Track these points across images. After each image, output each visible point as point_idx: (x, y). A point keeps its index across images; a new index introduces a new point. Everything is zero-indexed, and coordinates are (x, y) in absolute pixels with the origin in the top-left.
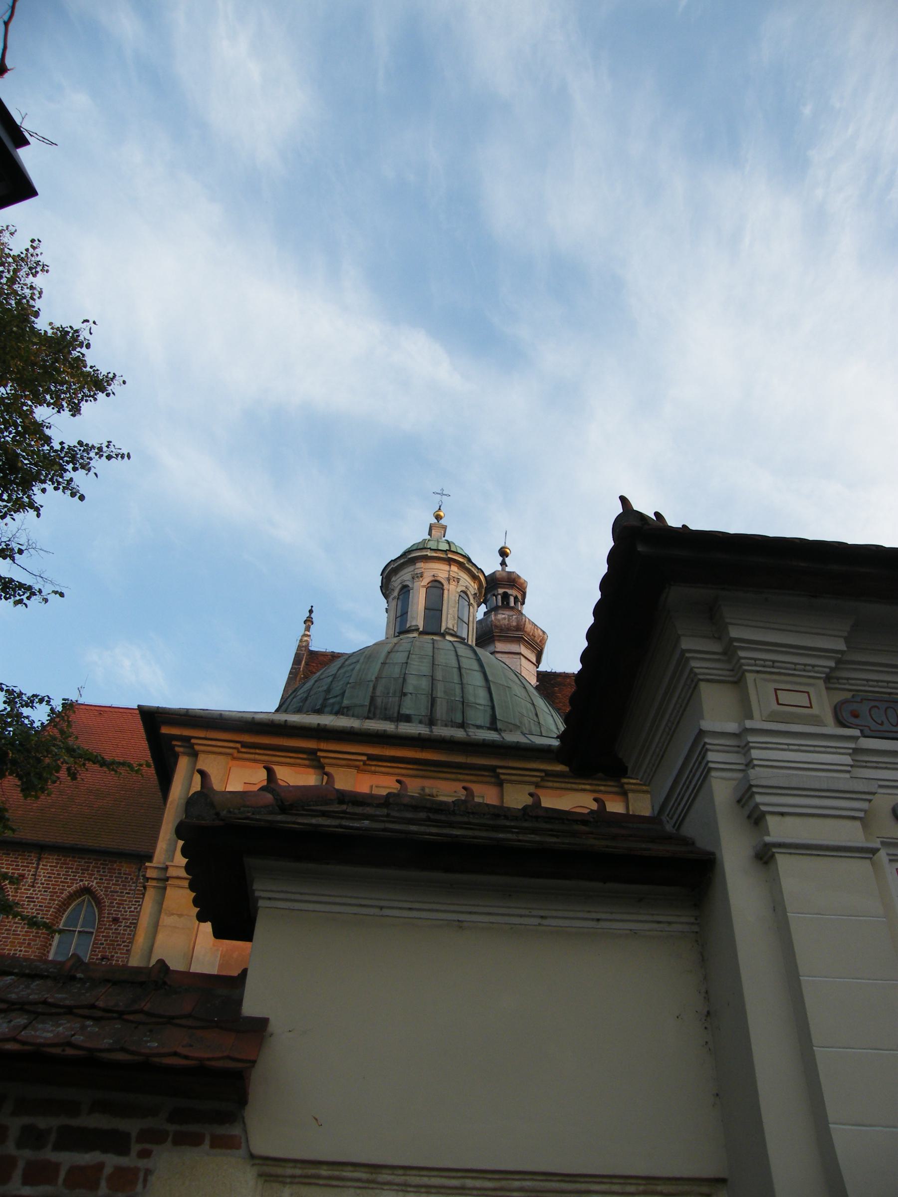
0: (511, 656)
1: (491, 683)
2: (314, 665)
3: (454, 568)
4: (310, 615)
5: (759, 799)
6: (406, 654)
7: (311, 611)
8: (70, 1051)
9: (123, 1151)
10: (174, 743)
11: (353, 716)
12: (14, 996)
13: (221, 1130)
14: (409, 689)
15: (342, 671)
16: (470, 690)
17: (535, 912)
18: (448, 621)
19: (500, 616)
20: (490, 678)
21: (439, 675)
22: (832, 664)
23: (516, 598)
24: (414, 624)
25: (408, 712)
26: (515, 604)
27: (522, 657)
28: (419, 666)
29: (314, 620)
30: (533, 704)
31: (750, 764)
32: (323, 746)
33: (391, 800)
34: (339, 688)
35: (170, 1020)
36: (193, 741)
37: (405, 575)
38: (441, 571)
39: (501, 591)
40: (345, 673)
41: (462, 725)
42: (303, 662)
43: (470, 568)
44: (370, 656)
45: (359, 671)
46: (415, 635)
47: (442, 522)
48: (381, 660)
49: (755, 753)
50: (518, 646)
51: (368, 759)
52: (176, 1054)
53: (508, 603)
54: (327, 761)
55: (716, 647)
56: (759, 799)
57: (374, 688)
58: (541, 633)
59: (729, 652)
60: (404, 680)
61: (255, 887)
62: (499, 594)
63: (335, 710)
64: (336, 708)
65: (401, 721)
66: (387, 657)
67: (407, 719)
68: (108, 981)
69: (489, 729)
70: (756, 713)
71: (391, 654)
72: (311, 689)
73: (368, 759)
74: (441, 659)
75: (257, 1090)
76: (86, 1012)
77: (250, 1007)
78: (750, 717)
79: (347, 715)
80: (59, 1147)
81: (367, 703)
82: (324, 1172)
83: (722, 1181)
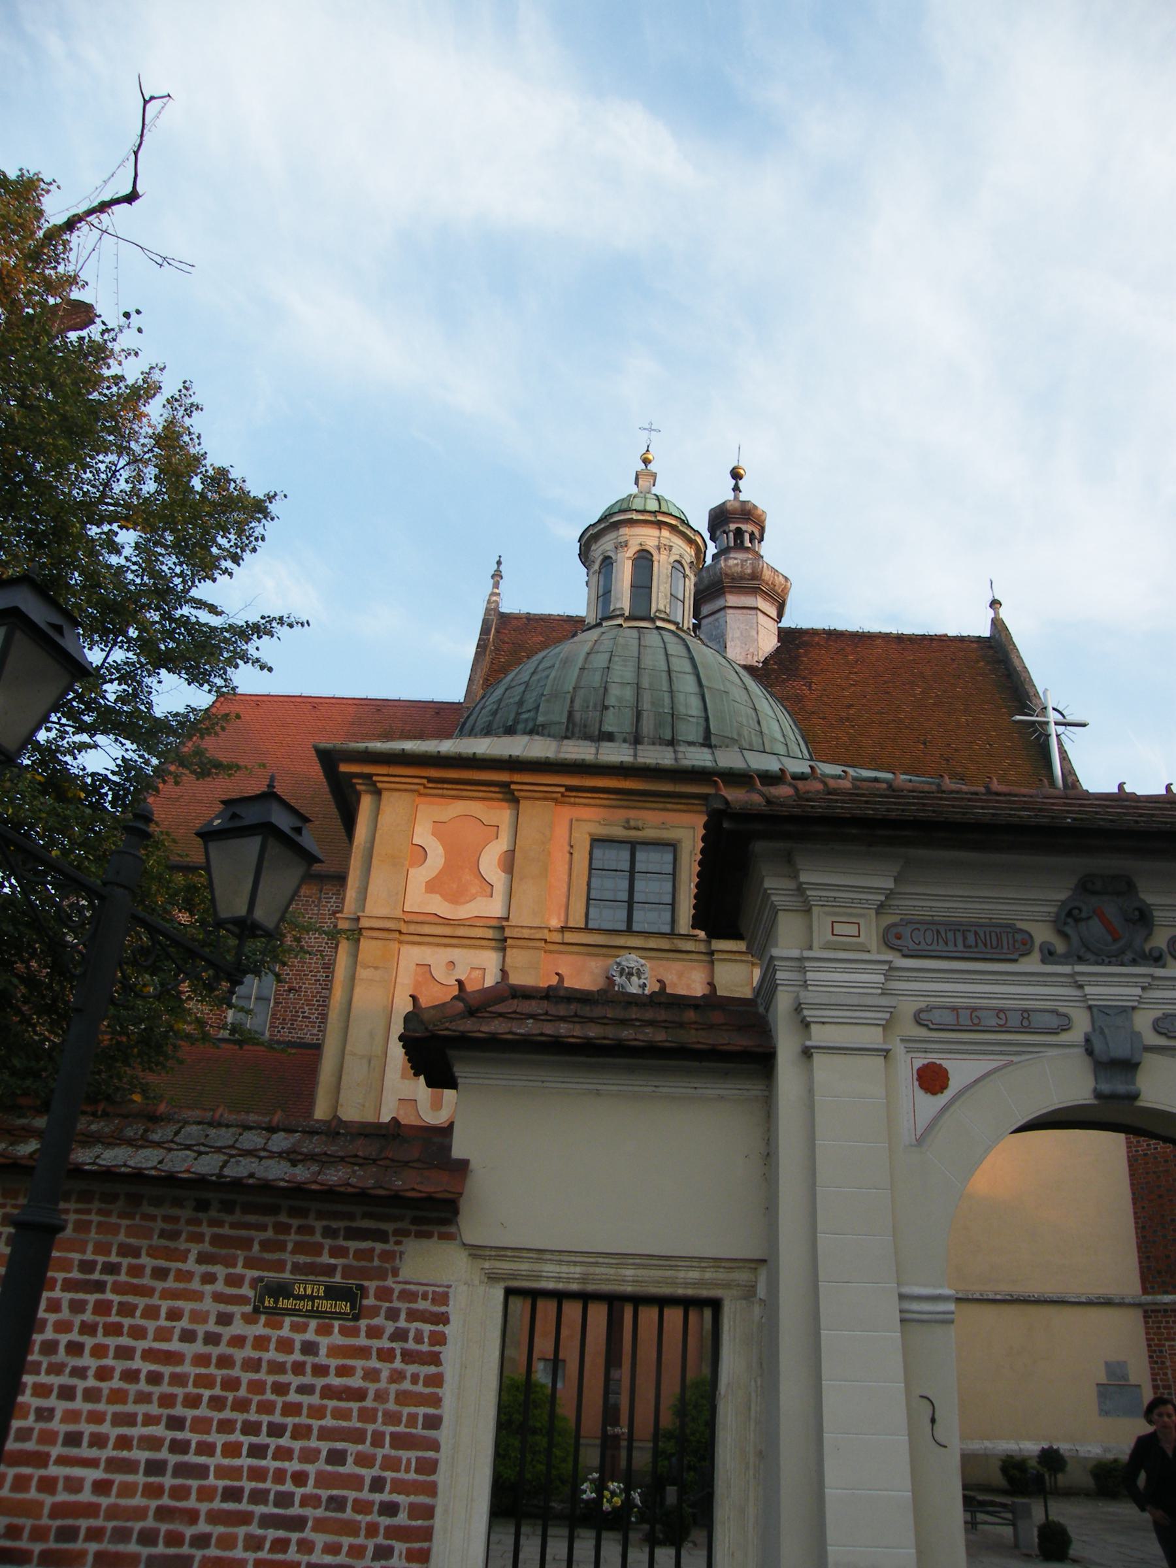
0: (745, 611)
1: (706, 690)
2: (507, 632)
3: (665, 533)
4: (498, 567)
5: (806, 1012)
6: (607, 656)
7: (499, 563)
8: (350, 1190)
9: (386, 1241)
10: (355, 781)
11: (549, 736)
12: (305, 1150)
13: (443, 1229)
14: (611, 701)
15: (535, 678)
16: (680, 698)
17: (650, 1083)
18: (660, 601)
19: (731, 562)
20: (704, 682)
21: (645, 683)
22: (882, 898)
23: (752, 535)
24: (618, 606)
25: (610, 729)
26: (751, 542)
27: (759, 612)
28: (623, 672)
29: (503, 574)
30: (755, 709)
31: (805, 985)
32: (517, 778)
33: (551, 993)
34: (531, 700)
35: (406, 1164)
36: (375, 778)
37: (606, 545)
38: (648, 537)
39: (733, 527)
40: (539, 681)
41: (672, 743)
42: (493, 630)
43: (685, 530)
44: (567, 658)
45: (555, 678)
46: (620, 621)
47: (651, 467)
48: (579, 665)
49: (810, 975)
50: (754, 599)
51: (566, 790)
52: (413, 1189)
53: (742, 542)
54: (522, 794)
55: (792, 885)
56: (806, 1012)
57: (572, 702)
58: (782, 580)
59: (800, 890)
60: (605, 688)
61: (455, 1069)
62: (730, 531)
63: (528, 729)
64: (530, 725)
65: (603, 740)
66: (586, 659)
67: (609, 737)
68: (361, 1134)
69: (703, 745)
70: (815, 945)
71: (592, 656)
72: (500, 701)
73: (567, 790)
74: (647, 662)
75: (464, 1206)
76: (352, 1160)
77: (457, 1152)
78: (810, 948)
79: (543, 735)
80: (346, 1238)
81: (564, 720)
82: (509, 1253)
83: (764, 1261)
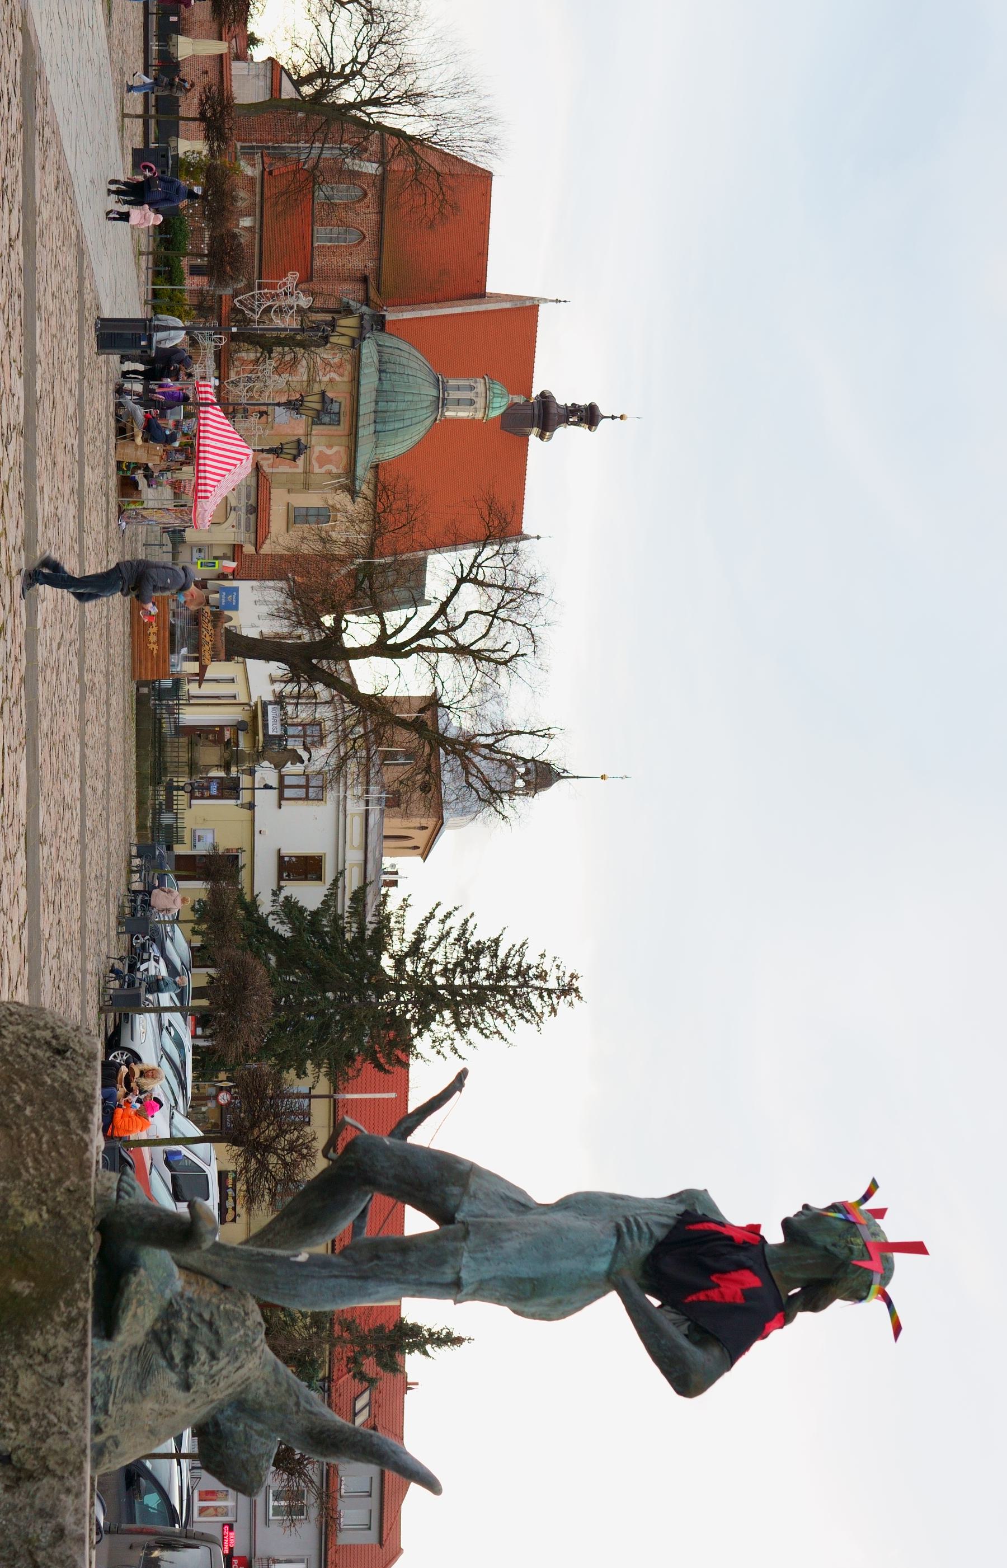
28: (402, 406)
74: (407, 412)
